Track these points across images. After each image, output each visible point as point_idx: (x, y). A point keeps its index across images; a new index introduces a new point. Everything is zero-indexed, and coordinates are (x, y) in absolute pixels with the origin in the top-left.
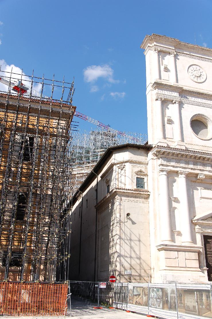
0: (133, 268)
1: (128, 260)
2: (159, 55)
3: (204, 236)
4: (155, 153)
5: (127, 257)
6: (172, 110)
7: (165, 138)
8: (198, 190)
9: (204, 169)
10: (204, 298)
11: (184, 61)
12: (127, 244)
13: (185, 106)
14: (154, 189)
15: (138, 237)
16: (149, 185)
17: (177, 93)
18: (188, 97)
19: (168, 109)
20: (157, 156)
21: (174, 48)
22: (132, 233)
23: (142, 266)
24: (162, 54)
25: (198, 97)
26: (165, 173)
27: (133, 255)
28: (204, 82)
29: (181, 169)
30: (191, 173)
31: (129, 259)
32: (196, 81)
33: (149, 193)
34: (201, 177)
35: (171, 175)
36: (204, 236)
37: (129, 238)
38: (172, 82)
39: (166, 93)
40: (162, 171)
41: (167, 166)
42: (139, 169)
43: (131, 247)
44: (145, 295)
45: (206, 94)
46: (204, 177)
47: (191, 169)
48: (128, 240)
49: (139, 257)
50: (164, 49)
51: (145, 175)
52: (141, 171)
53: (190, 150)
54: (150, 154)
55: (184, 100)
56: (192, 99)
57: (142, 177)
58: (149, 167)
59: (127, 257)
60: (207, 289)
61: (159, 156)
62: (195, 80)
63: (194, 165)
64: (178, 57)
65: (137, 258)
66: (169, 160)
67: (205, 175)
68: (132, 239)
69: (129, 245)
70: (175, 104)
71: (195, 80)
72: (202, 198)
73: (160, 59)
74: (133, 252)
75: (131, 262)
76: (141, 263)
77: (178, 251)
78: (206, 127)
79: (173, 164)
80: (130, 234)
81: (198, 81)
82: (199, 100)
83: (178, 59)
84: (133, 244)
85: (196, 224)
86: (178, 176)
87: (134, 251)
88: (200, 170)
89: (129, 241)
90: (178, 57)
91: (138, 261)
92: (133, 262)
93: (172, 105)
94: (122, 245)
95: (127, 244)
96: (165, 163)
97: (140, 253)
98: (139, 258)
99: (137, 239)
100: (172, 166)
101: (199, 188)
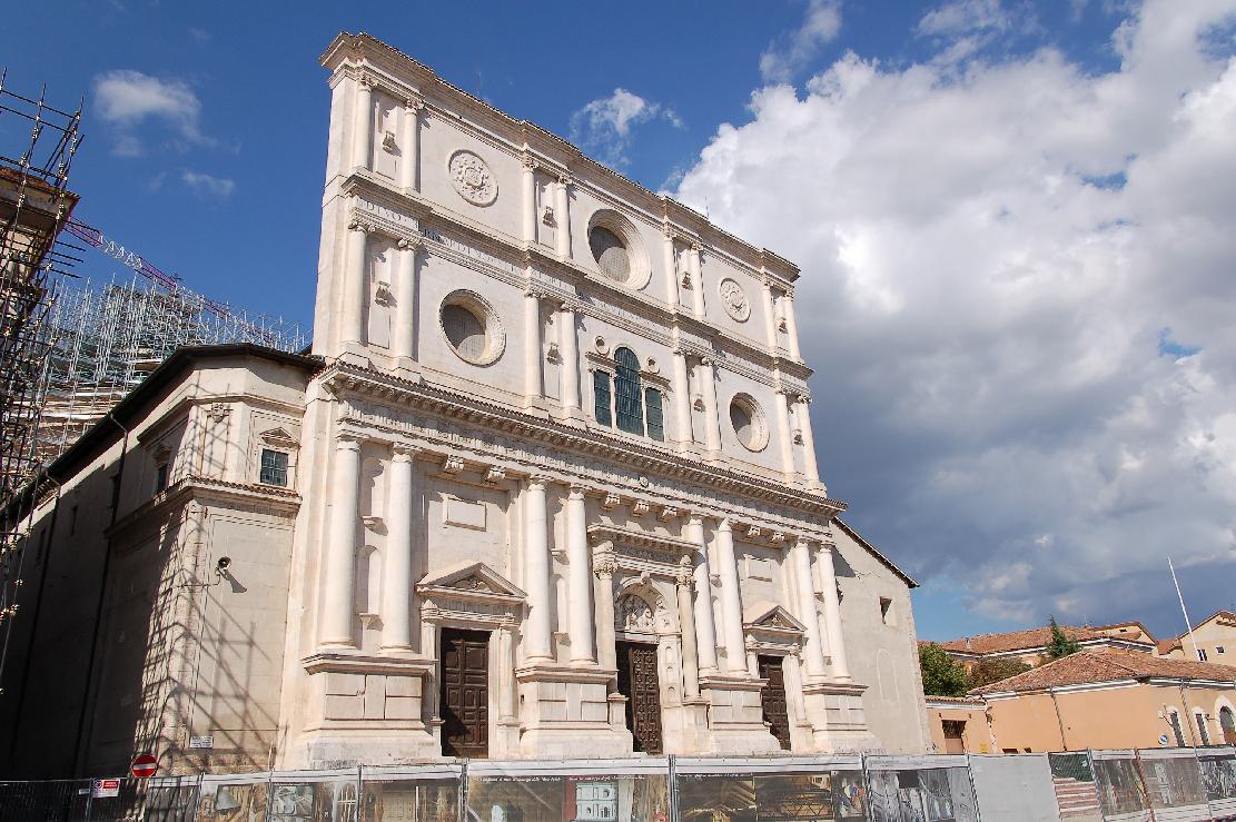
0: (219, 726)
1: (207, 703)
2: (373, 101)
3: (445, 631)
4: (332, 382)
6: (395, 268)
7: (364, 341)
9: (465, 445)
10: (441, 803)
11: (444, 134)
12: (209, 655)
14: (315, 489)
15: (248, 632)
16: (301, 476)
20: (335, 391)
22: (229, 620)
23: (248, 722)
24: (384, 98)
25: (470, 245)
26: (353, 445)
27: (225, 687)
28: (490, 204)
29: (400, 438)
30: (426, 453)
31: (211, 700)
32: (470, 198)
33: (297, 501)
35: (371, 455)
36: (445, 631)
37: (216, 636)
38: (403, 184)
39: (383, 212)
40: (346, 438)
41: (364, 425)
42: (276, 425)
43: (221, 663)
44: (257, 809)
45: (490, 240)
46: (462, 466)
47: (428, 438)
48: (212, 640)
50: (388, 86)
51: (291, 445)
52: (280, 433)
53: (433, 386)
54: (316, 386)
55: (429, 244)
56: (456, 246)
57: (282, 450)
58: (309, 422)
59: (202, 693)
60: (450, 775)
61: (342, 393)
63: (440, 431)
65: (237, 697)
67: (466, 462)
68: (227, 637)
69: (215, 655)
70: (403, 252)
71: (467, 193)
72: (448, 523)
74: (224, 678)
77: (366, 674)
78: (481, 329)
80: (224, 624)
81: (474, 200)
82: (474, 253)
83: (428, 126)
84: (227, 653)
85: (424, 597)
87: (230, 676)
89: (217, 644)
90: (428, 120)
91: (238, 706)
92: (223, 710)
94: (190, 657)
95: (209, 655)
96: (356, 415)
98: (244, 697)
99: (244, 638)
100: (377, 426)
101: (444, 496)
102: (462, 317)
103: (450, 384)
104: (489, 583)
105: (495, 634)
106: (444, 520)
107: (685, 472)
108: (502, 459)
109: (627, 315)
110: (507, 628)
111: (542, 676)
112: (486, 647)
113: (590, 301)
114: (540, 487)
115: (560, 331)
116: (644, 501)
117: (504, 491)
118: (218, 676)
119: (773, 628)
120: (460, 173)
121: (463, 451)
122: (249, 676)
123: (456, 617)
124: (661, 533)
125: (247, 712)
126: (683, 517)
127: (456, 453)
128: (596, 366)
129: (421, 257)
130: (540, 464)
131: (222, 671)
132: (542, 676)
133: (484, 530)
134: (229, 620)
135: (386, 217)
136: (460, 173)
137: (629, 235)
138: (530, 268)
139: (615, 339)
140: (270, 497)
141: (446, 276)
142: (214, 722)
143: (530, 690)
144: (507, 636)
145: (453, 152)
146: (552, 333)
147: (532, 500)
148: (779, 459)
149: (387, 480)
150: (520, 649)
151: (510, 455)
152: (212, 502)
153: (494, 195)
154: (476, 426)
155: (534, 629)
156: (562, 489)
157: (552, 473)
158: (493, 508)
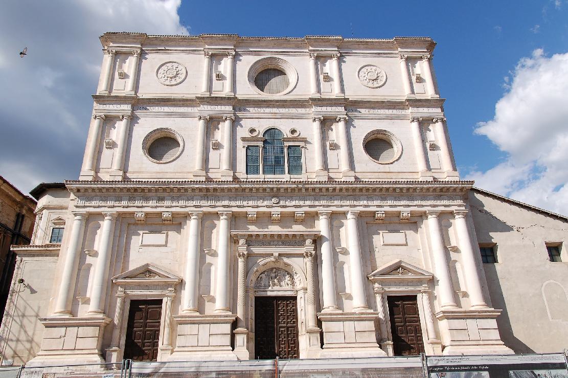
0: (17, 355)
2: (316, 64)
3: (389, 297)
5: (12, 340)
6: (338, 132)
11: (352, 63)
12: (17, 323)
13: (356, 122)
15: (36, 310)
17: (230, 107)
18: (148, 108)
21: (337, 49)
22: (28, 307)
23: (32, 352)
24: (122, 56)
25: (165, 106)
26: (78, 217)
27: (23, 337)
28: (383, 85)
31: (15, 343)
32: (372, 86)
34: (379, 215)
36: (389, 297)
37: (20, 314)
40: (75, 215)
42: (56, 216)
43: (22, 326)
45: (174, 100)
46: (384, 215)
47: (121, 207)
48: (19, 316)
49: (30, 339)
52: (60, 219)
53: (135, 180)
59: (12, 340)
62: (370, 85)
63: (129, 200)
64: (147, 56)
65: (28, 341)
66: (89, 199)
68: (26, 314)
71: (370, 85)
73: (319, 66)
74: (23, 332)
75: (16, 347)
76: (32, 347)
79: (93, 203)
80: (25, 308)
82: (166, 109)
83: (344, 62)
84: (25, 321)
85: (374, 282)
86: (219, 219)
87: (25, 332)
88: (138, 207)
89: (21, 318)
90: (344, 59)
91: (28, 345)
92: (20, 347)
93: (337, 124)
94: (7, 324)
95: (17, 323)
96: (81, 203)
98: (31, 341)
99: (34, 314)
100: (93, 206)
101: (141, 232)
103: (373, 178)
104: (409, 271)
105: (419, 296)
106: (382, 243)
108: (404, 208)
109: (275, 110)
110: (425, 292)
111: (449, 316)
112: (416, 304)
113: (146, 109)
114: (324, 216)
115: (337, 133)
116: (276, 211)
117: (414, 222)
118: (20, 331)
119: (400, 276)
120: (364, 77)
121: (381, 207)
122: (34, 331)
124: (298, 229)
125: (32, 347)
126: (314, 216)
127: (140, 210)
129: (348, 123)
130: (427, 205)
131: (22, 330)
132: (449, 316)
133: (406, 245)
134: (28, 307)
136: (364, 77)
138: (410, 108)
139: (261, 126)
140: (48, 249)
141: (363, 128)
142: (15, 353)
143: (444, 325)
144: (425, 296)
145: (358, 70)
147: (431, 224)
149: (346, 229)
150: (436, 303)
151: (174, 204)
152: (25, 255)
153: (384, 80)
154: (150, 194)
155: (443, 291)
156: (450, 214)
157: (88, 210)
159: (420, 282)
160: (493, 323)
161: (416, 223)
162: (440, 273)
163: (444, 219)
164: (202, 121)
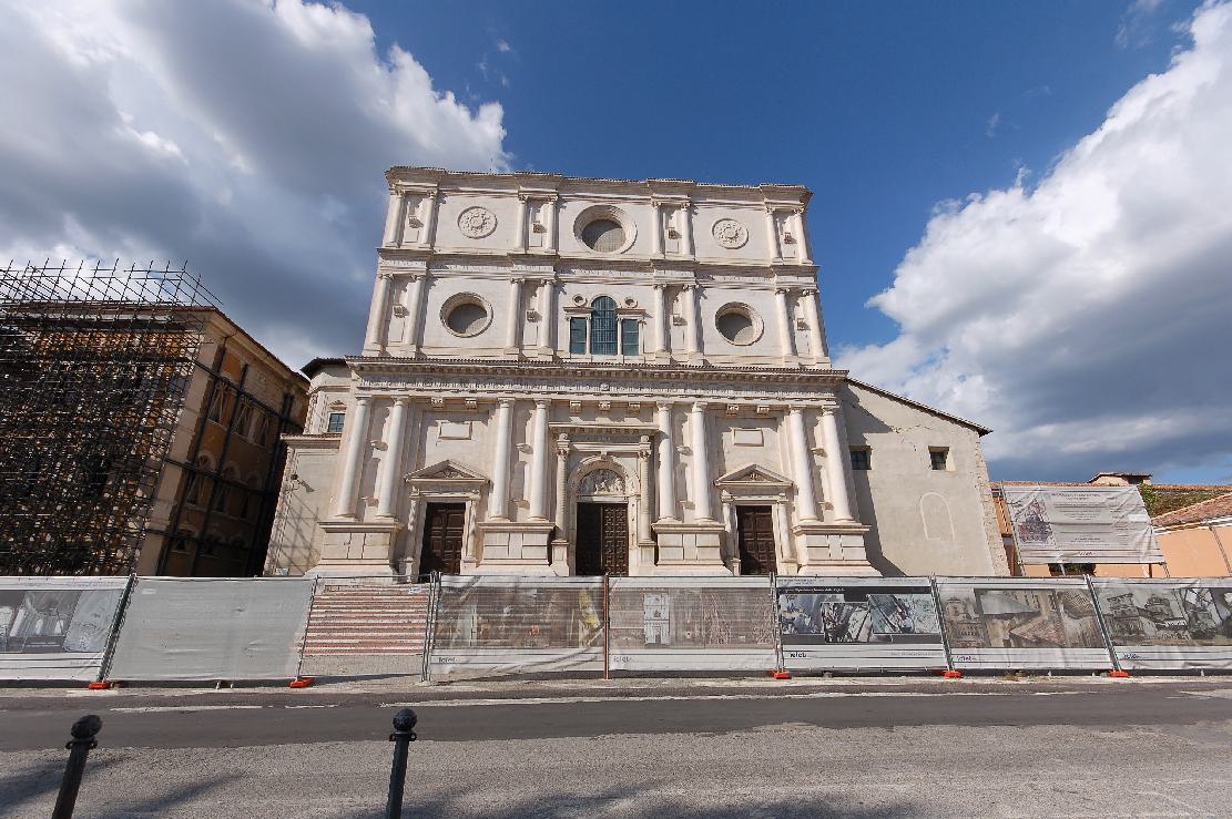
1: (288, 551)
5: (286, 546)
6: (685, 302)
8: (436, 425)
11: (706, 216)
13: (707, 292)
19: (406, 291)
24: (414, 199)
26: (362, 402)
27: (299, 542)
38: (684, 253)
39: (402, 264)
40: (359, 399)
47: (416, 390)
52: (339, 403)
56: (578, 273)
59: (286, 546)
62: (728, 244)
64: (445, 199)
65: (306, 548)
74: (299, 536)
78: (749, 322)
83: (696, 214)
84: (302, 524)
85: (721, 488)
87: (303, 537)
92: (297, 554)
96: (367, 384)
97: (312, 539)
98: (309, 548)
100: (378, 389)
101: (439, 422)
102: (733, 321)
104: (766, 477)
105: (774, 507)
107: (686, 375)
108: (762, 400)
110: (782, 503)
111: (809, 531)
115: (684, 305)
116: (605, 401)
117: (774, 418)
123: (745, 499)
124: (632, 422)
126: (653, 407)
128: (571, 315)
129: (698, 293)
130: (792, 398)
132: (809, 531)
135: (673, 276)
137: (619, 217)
139: (590, 292)
141: (718, 297)
143: (801, 541)
144: (781, 507)
146: (799, 312)
147: (794, 421)
148: (777, 346)
150: (794, 514)
152: (298, 446)
155: (803, 503)
158: (767, 430)
159: (775, 491)
160: (860, 541)
161: (775, 419)
162: (801, 479)
163: (810, 416)
164: (515, 285)
